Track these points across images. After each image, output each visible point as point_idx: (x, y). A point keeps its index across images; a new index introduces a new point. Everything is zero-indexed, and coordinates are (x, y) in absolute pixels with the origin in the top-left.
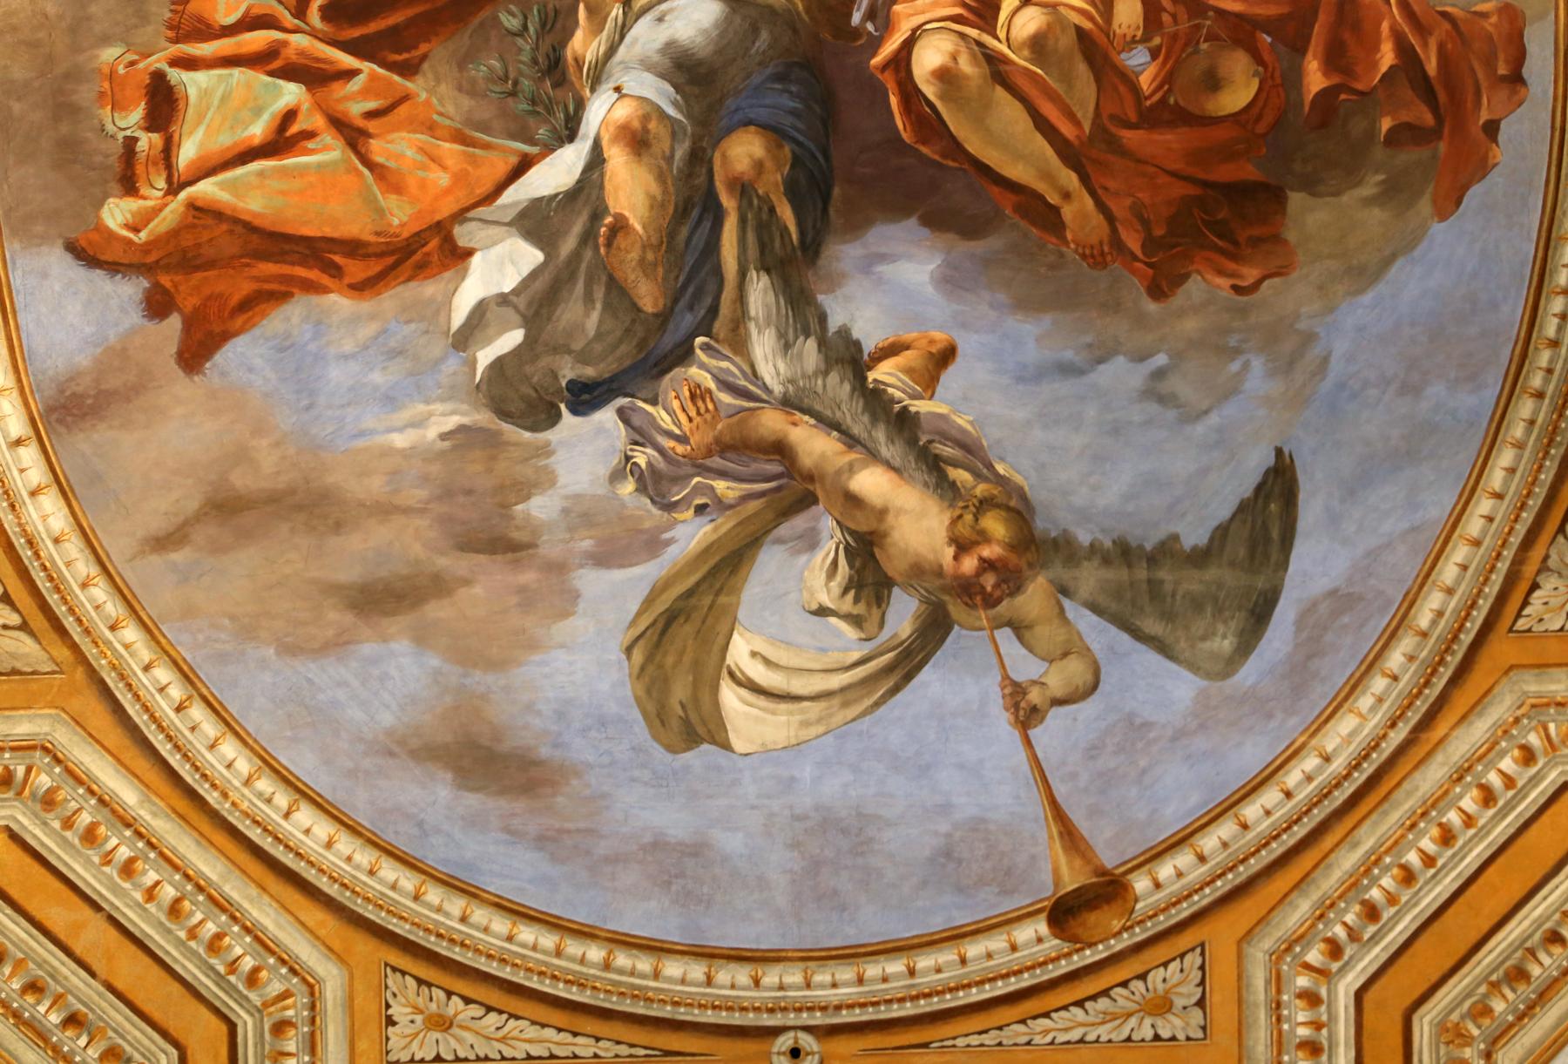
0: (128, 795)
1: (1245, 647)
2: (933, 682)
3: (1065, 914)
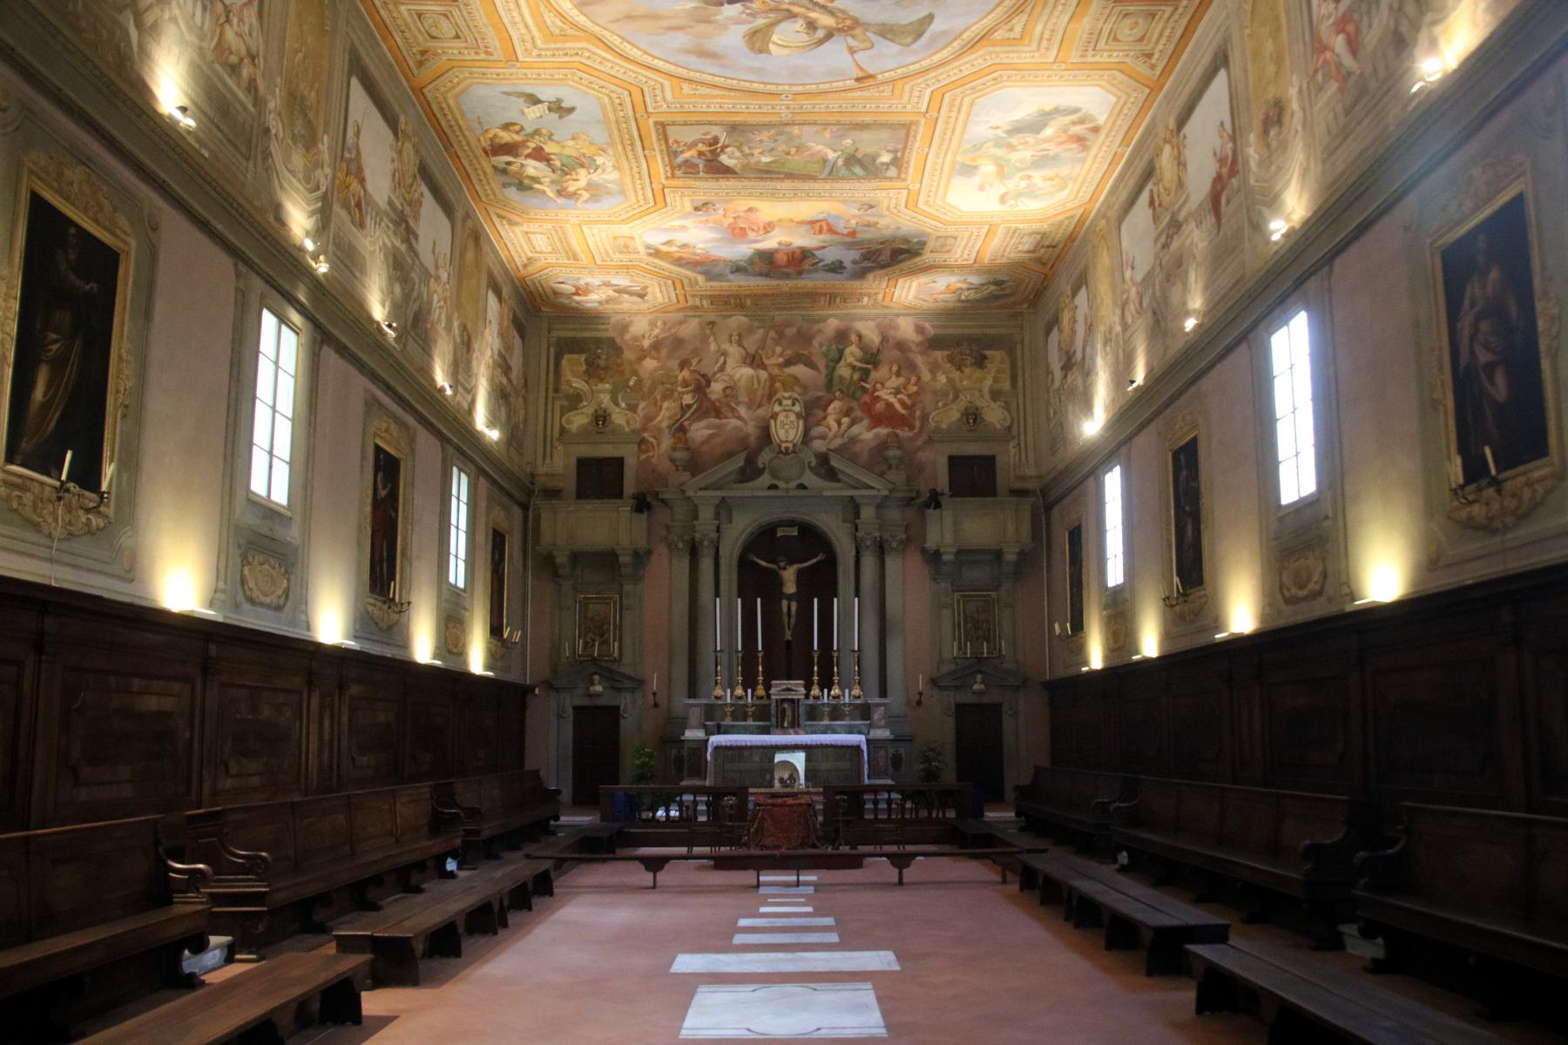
0: (610, 57)
1: (915, 40)
2: (827, 45)
3: (858, 80)
